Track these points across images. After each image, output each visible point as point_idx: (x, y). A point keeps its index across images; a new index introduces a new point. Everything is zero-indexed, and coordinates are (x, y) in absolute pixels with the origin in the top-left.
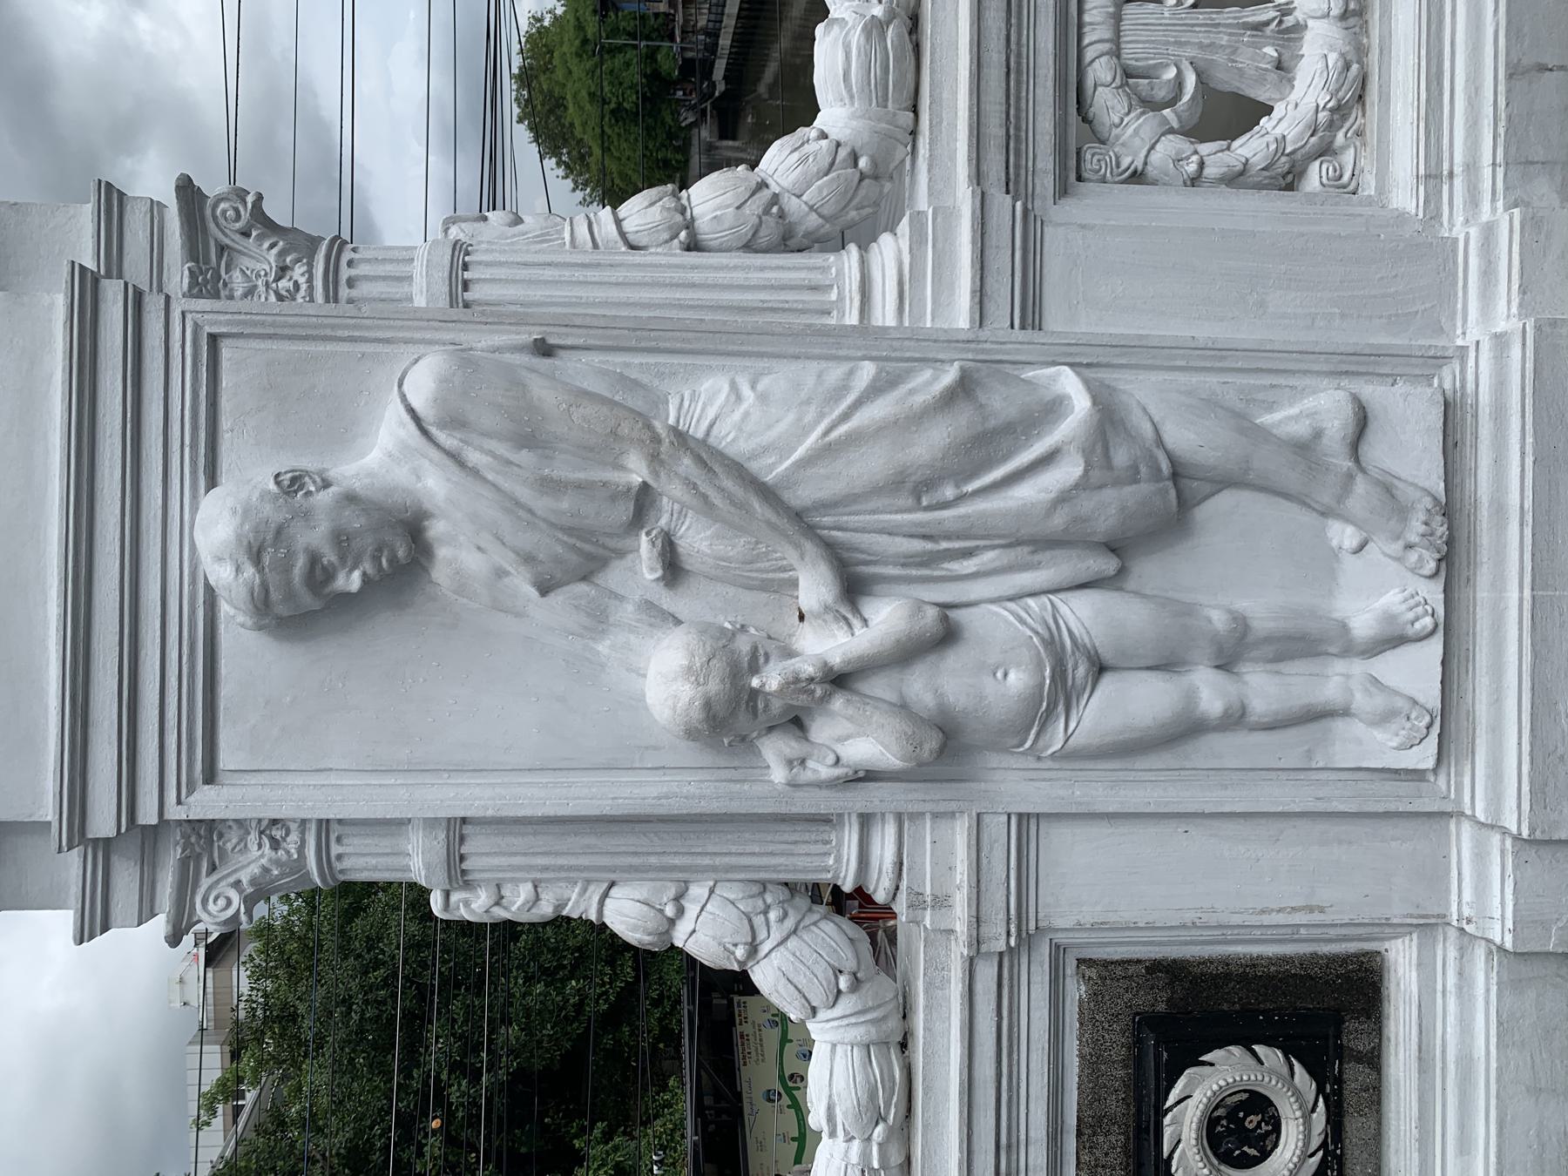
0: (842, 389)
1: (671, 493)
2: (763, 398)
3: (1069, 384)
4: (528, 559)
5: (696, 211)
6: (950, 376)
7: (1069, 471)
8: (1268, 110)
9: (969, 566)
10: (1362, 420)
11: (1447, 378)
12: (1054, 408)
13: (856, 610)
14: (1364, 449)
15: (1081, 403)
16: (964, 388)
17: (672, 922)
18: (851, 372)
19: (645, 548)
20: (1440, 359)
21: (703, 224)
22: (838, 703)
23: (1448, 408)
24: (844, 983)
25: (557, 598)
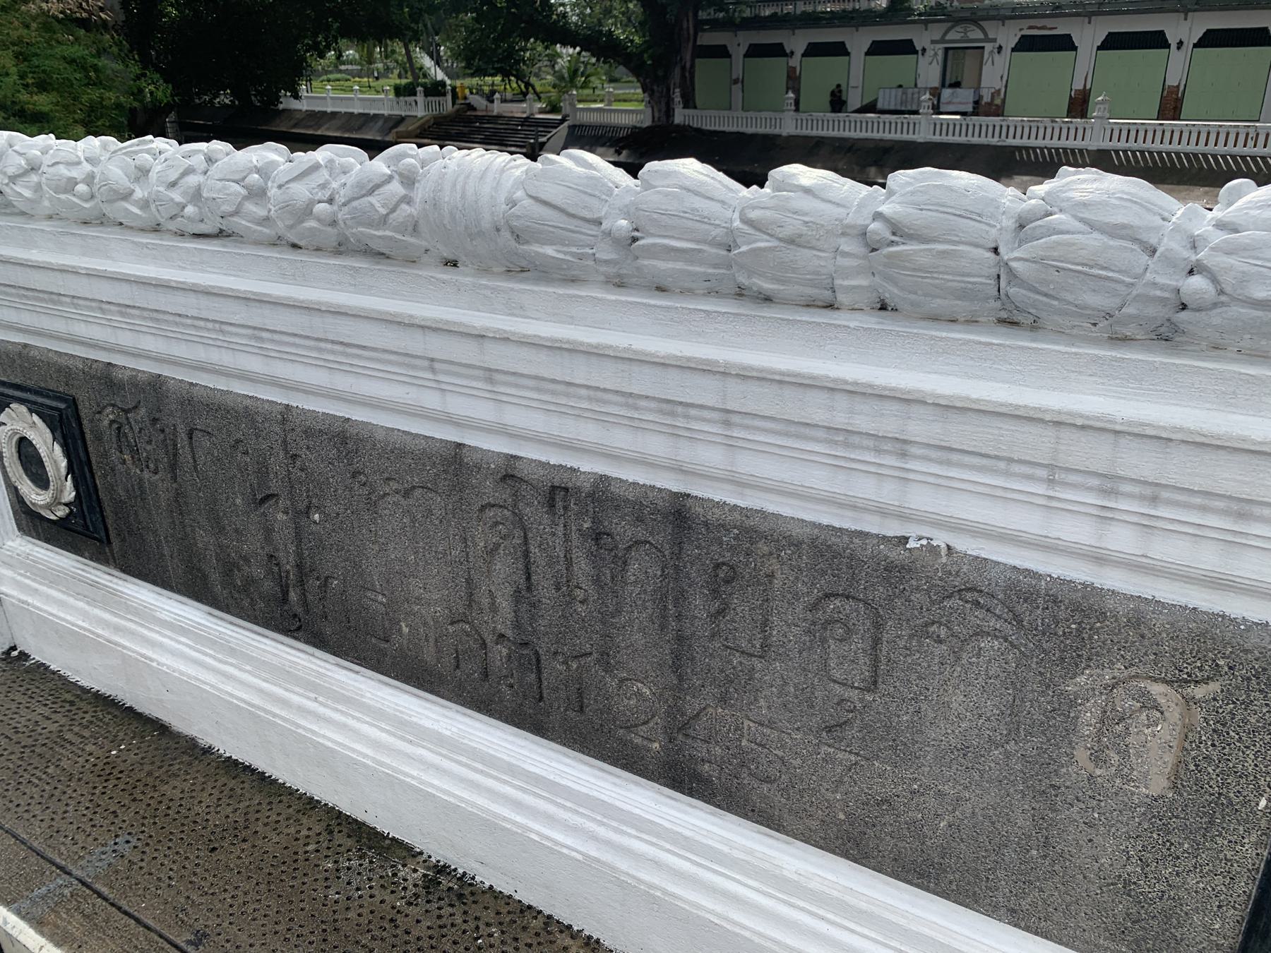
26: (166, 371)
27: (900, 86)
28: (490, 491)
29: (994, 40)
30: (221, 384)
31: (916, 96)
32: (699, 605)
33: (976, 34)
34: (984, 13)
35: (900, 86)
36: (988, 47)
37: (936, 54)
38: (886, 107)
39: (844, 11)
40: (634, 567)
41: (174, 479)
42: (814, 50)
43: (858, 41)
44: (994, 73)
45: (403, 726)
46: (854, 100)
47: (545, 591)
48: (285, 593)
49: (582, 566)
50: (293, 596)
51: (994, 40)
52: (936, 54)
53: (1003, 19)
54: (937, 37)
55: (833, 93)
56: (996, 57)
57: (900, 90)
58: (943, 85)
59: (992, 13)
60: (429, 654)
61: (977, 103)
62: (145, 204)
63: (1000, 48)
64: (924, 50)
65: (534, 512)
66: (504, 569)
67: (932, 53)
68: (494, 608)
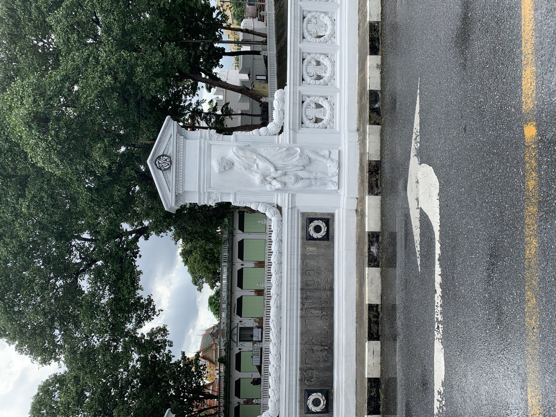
1: (258, 161)
2: (267, 151)
3: (298, 149)
4: (244, 167)
6: (286, 148)
8: (323, 120)
9: (289, 168)
10: (330, 153)
12: (297, 152)
14: (331, 156)
15: (299, 151)
16: (287, 149)
19: (255, 166)
21: (261, 134)
22: (274, 180)
23: (339, 151)
25: (247, 171)
26: (298, 368)
27: (252, 357)
28: (304, 312)
29: (238, 324)
30: (299, 356)
31: (256, 350)
32: (311, 287)
33: (235, 331)
34: (229, 328)
35: (252, 357)
36: (240, 326)
37: (241, 345)
38: (259, 361)
39: (224, 382)
40: (308, 295)
41: (313, 369)
42: (238, 394)
43: (236, 375)
44: (248, 323)
45: (339, 329)
46: (257, 375)
47: (314, 306)
48: (326, 350)
49: (310, 301)
50: (326, 348)
51: (238, 324)
52: (241, 345)
53: (231, 321)
54: (236, 344)
55: (254, 384)
56: (243, 323)
57: (254, 357)
58: (252, 341)
59: (229, 326)
60: (327, 324)
61: (258, 327)
62: (277, 366)
63: (240, 321)
64: (240, 349)
65: (305, 307)
66: (313, 311)
67: (241, 346)
68: (318, 313)
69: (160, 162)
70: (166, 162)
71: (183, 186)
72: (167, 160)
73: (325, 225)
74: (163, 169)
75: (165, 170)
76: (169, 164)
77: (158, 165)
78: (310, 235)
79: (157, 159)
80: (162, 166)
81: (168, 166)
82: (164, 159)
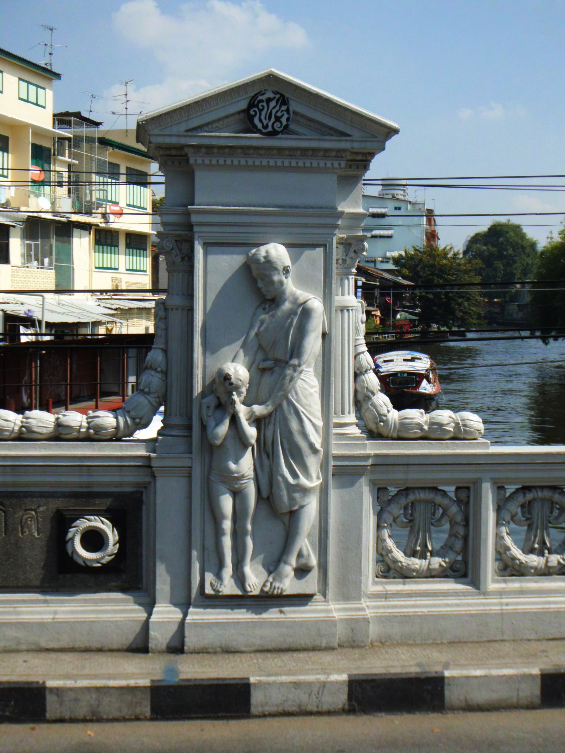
0: (315, 417)
5: (366, 375)
7: (291, 480)
11: (318, 597)
13: (254, 421)
17: (155, 370)
18: (319, 419)
20: (324, 595)
24: (137, 420)
69: (272, 104)
70: (273, 119)
71: (210, 167)
72: (277, 124)
73: (104, 561)
74: (252, 113)
75: (251, 118)
76: (266, 127)
77: (263, 98)
78: (77, 519)
79: (282, 96)
80: (260, 111)
81: (260, 126)
82: (279, 114)
